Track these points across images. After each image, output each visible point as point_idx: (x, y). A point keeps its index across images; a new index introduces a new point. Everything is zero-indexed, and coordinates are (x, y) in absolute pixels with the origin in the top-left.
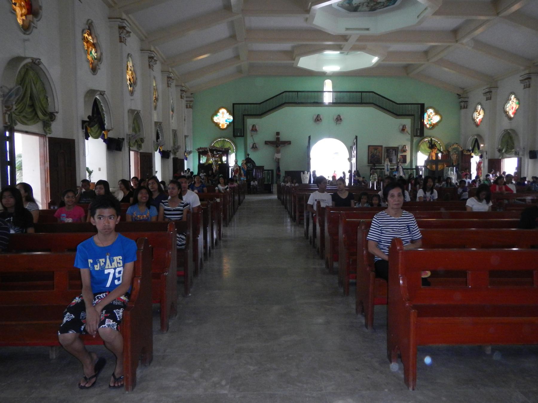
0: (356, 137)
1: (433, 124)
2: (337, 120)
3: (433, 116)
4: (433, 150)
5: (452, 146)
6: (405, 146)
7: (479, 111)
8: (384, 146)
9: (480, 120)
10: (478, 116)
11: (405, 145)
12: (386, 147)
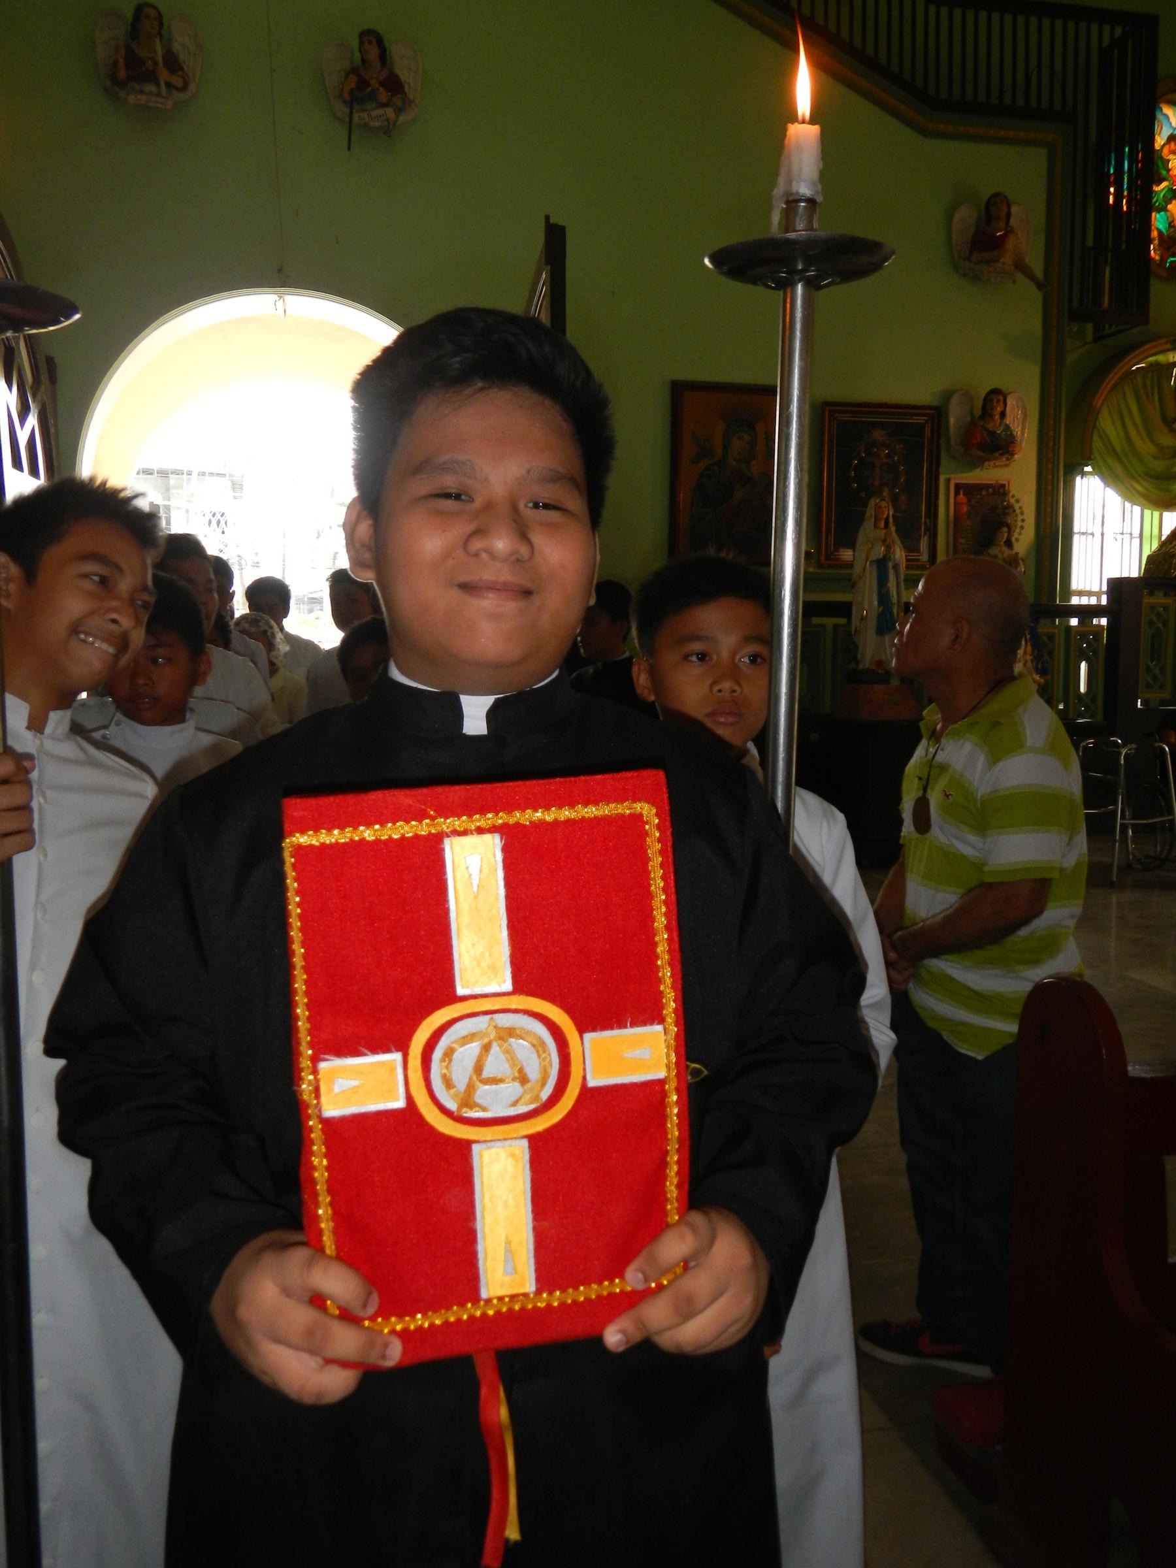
0: (555, 237)
2: (353, 81)
6: (996, 396)
11: (1004, 389)
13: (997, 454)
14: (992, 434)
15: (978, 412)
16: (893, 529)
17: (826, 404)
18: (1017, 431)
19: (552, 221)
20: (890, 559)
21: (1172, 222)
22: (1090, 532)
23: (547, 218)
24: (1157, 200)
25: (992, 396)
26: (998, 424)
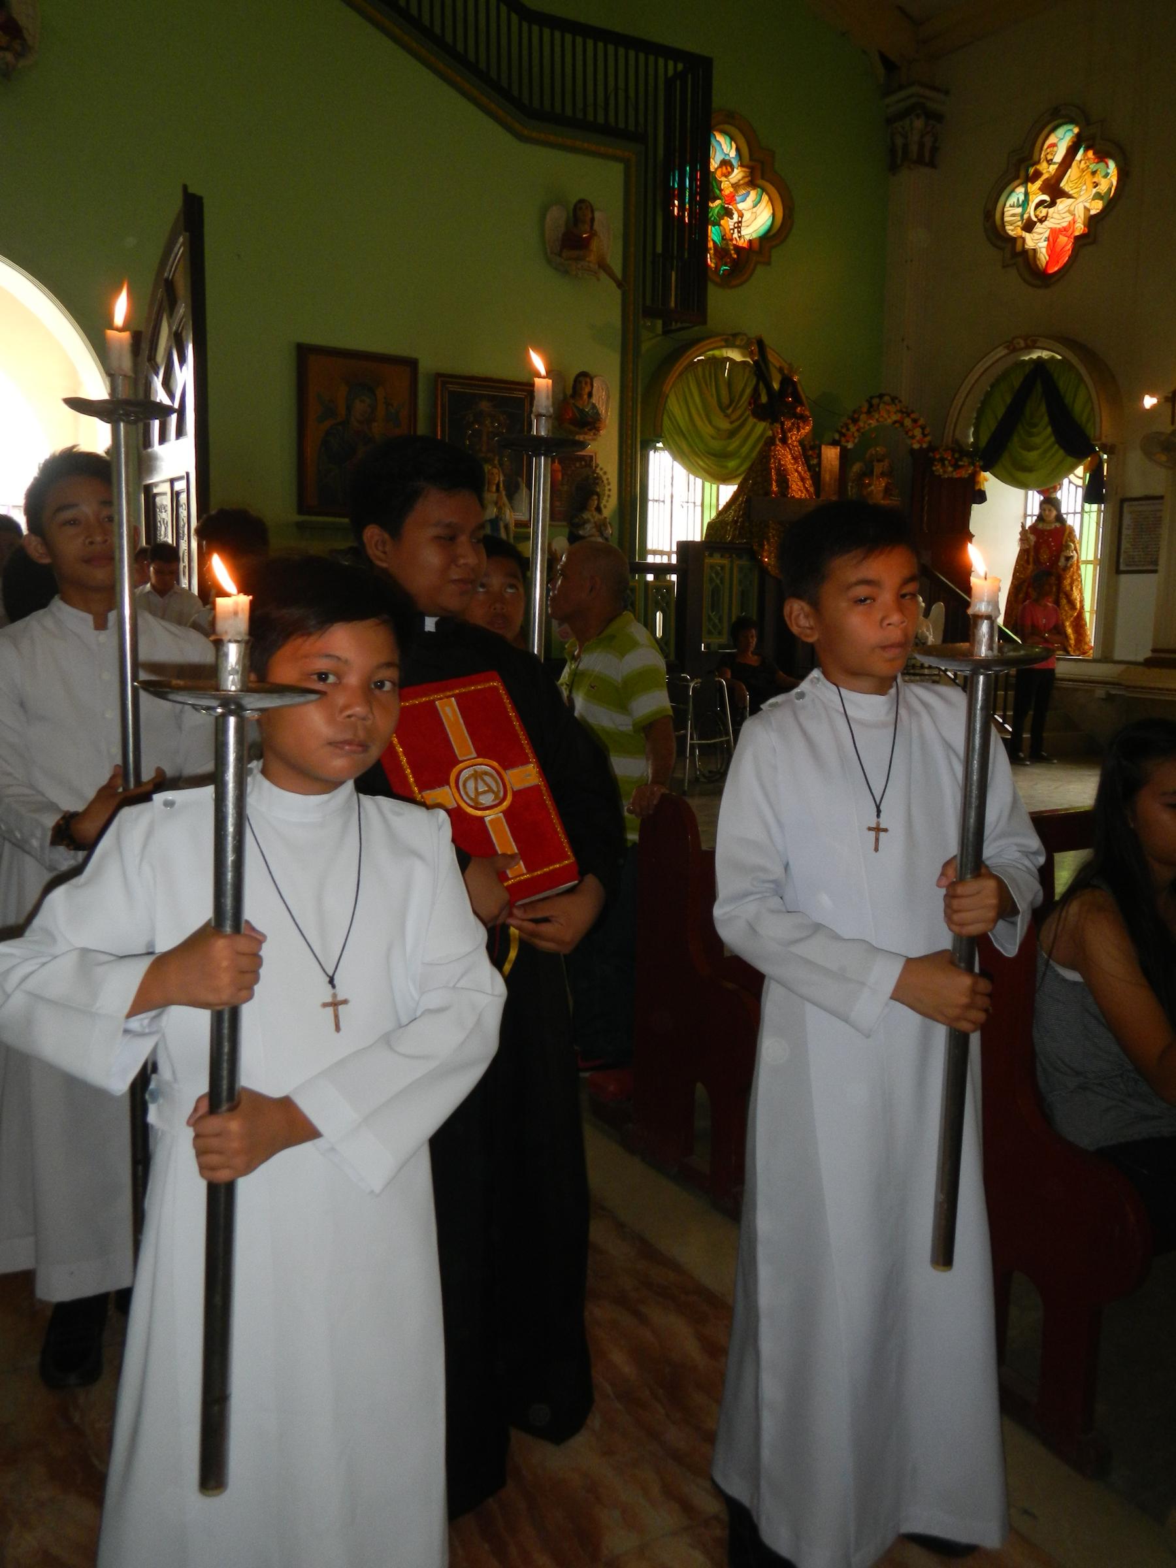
1: (738, 249)
3: (736, 186)
4: (788, 424)
5: (863, 417)
6: (584, 378)
7: (1048, 170)
8: (428, 364)
9: (1054, 234)
10: (1043, 212)
12: (442, 379)
13: (586, 430)
14: (582, 411)
15: (569, 392)
16: (504, 493)
17: (439, 375)
18: (602, 410)
19: (191, 190)
20: (501, 519)
21: (725, 235)
22: (662, 499)
23: (185, 187)
24: (713, 215)
25: (581, 378)
26: (586, 403)
